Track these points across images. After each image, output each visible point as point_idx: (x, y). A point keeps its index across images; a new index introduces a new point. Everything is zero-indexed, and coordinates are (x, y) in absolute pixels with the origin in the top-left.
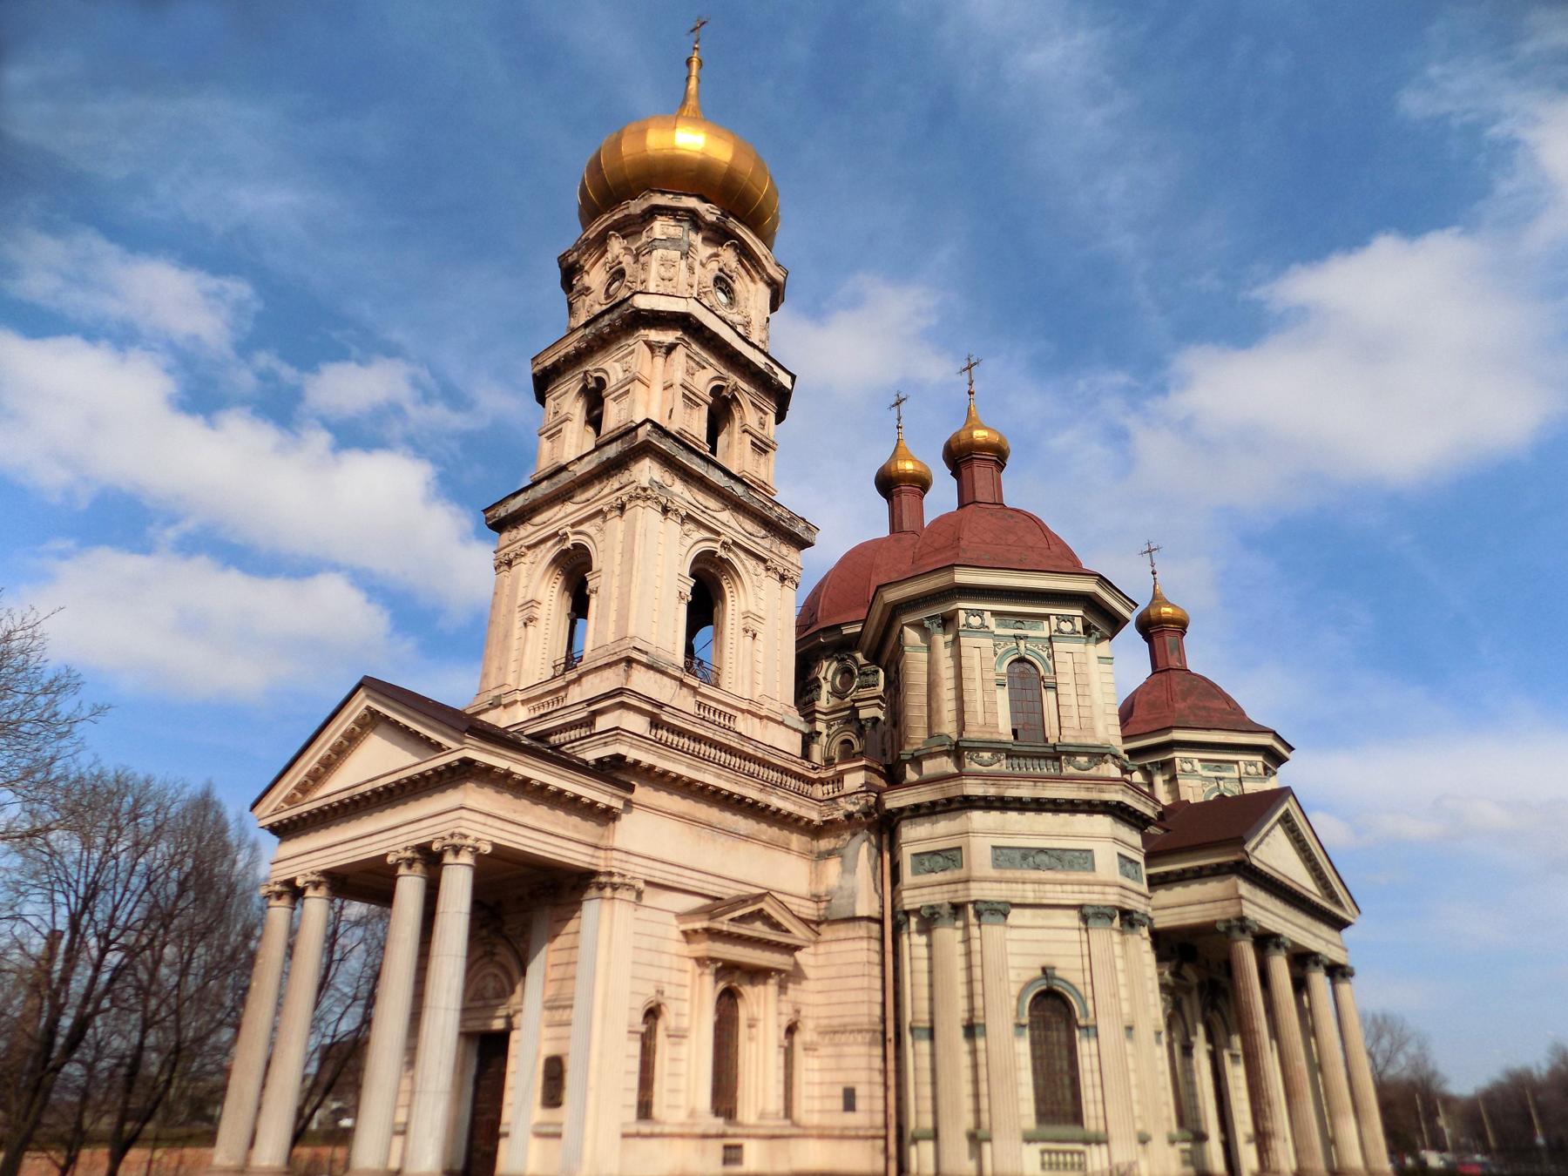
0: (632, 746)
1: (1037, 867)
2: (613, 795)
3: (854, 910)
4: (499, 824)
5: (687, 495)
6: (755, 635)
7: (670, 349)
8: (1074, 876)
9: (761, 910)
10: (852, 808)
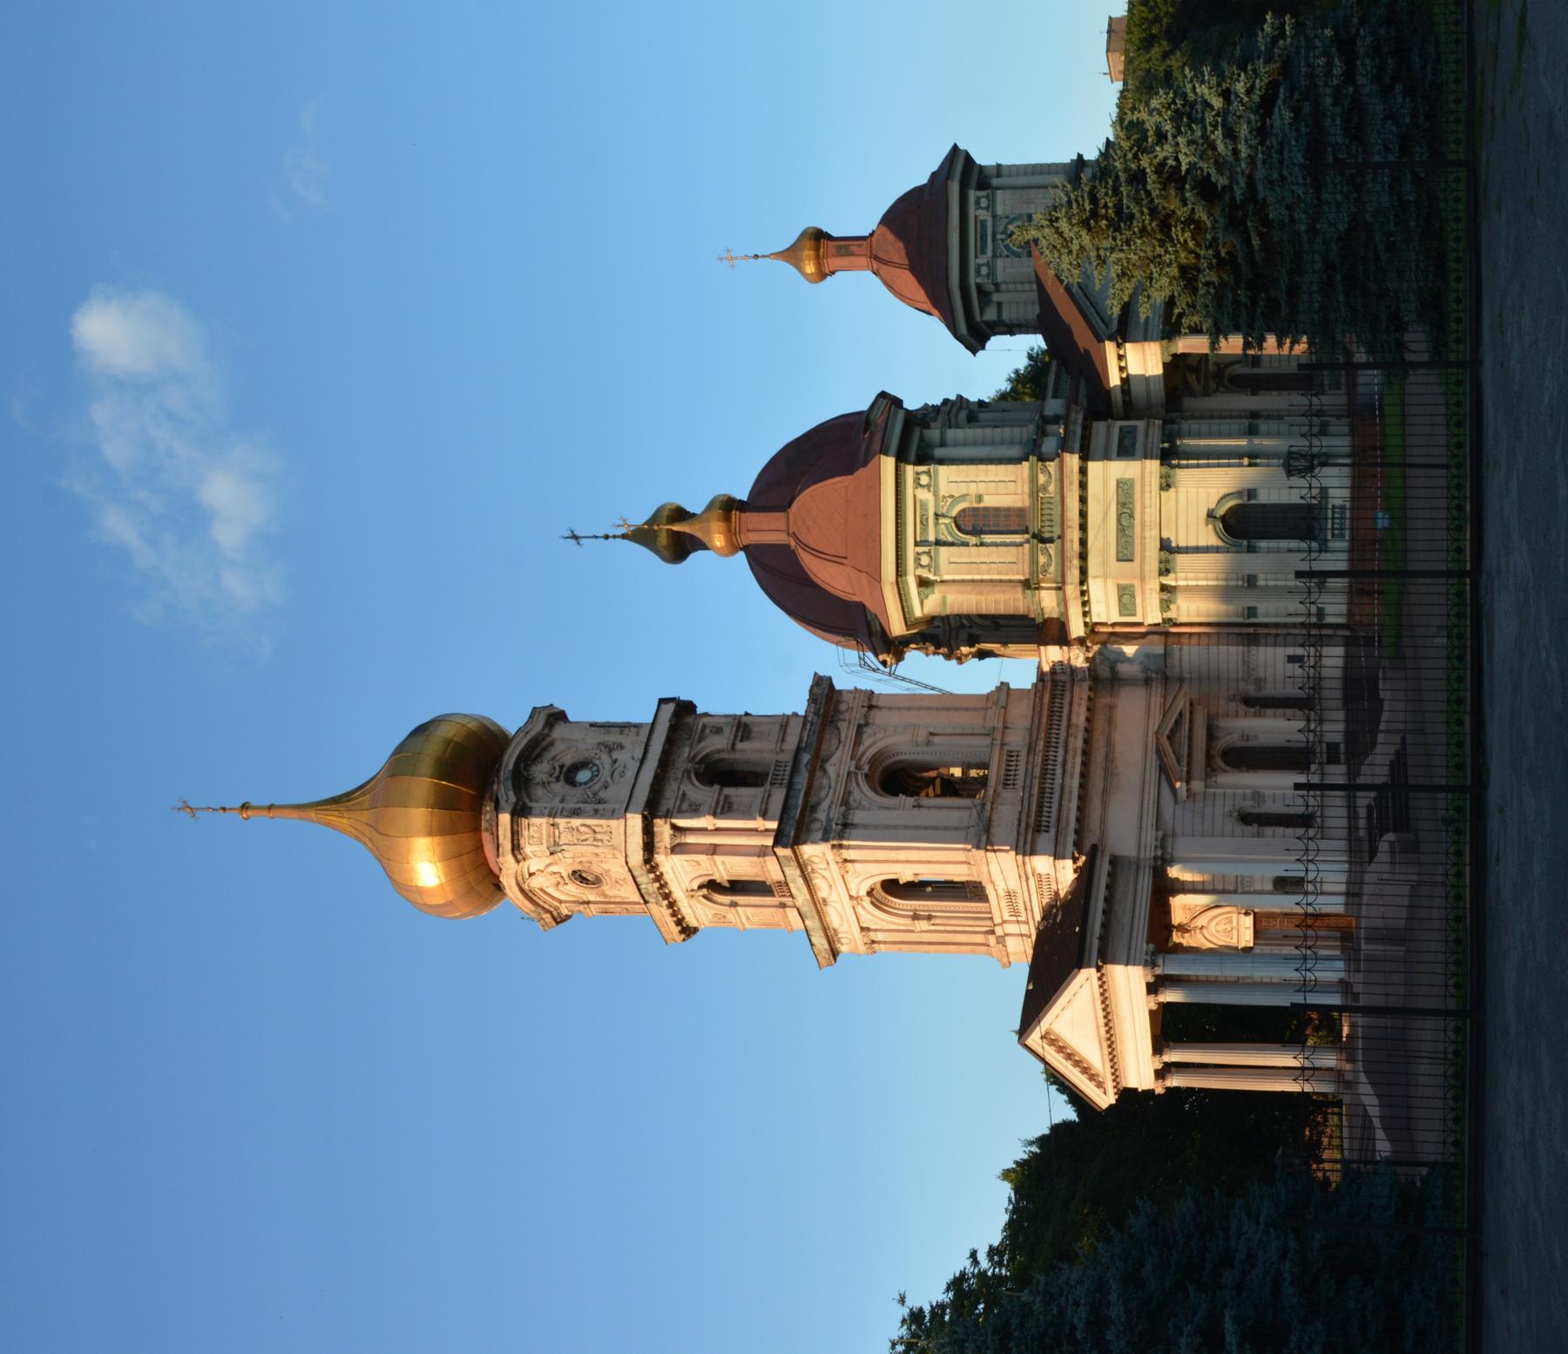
2: (1102, 861)
3: (1159, 655)
4: (1134, 940)
5: (825, 805)
6: (931, 734)
9: (1168, 737)
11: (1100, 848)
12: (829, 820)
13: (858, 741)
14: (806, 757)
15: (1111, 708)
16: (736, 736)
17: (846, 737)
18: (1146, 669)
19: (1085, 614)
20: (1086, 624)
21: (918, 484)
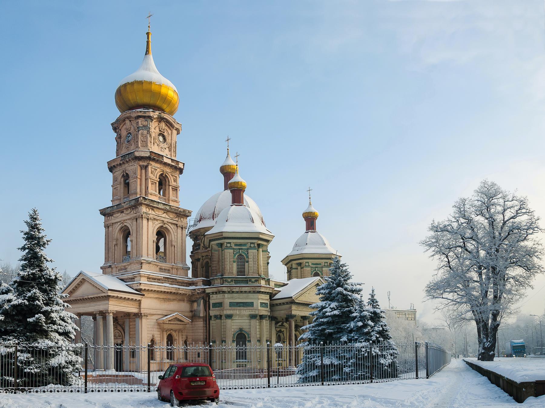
0: (144, 286)
1: (240, 306)
4: (116, 307)
5: (153, 213)
6: (174, 246)
7: (146, 167)
8: (249, 308)
10: (198, 292)
11: (144, 297)
12: (149, 214)
13: (171, 223)
14: (168, 208)
15: (183, 300)
16: (173, 186)
17: (173, 220)
18: (194, 311)
19: (213, 293)
20: (209, 293)
21: (251, 243)
